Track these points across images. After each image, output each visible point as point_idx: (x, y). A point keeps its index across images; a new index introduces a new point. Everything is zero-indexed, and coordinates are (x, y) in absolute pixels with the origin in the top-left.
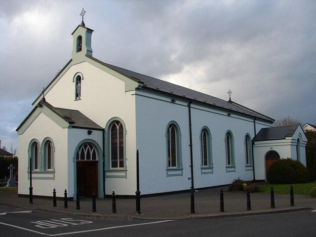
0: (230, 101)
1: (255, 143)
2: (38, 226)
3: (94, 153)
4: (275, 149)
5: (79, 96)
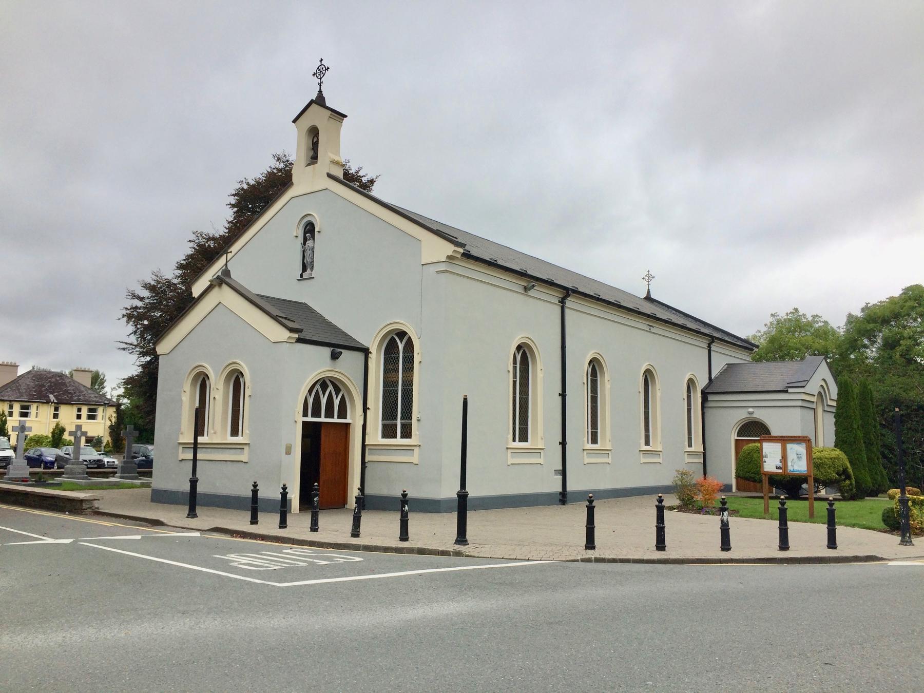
0: (648, 298)
1: (710, 398)
2: (232, 564)
3: (343, 403)
4: (761, 415)
5: (309, 271)
